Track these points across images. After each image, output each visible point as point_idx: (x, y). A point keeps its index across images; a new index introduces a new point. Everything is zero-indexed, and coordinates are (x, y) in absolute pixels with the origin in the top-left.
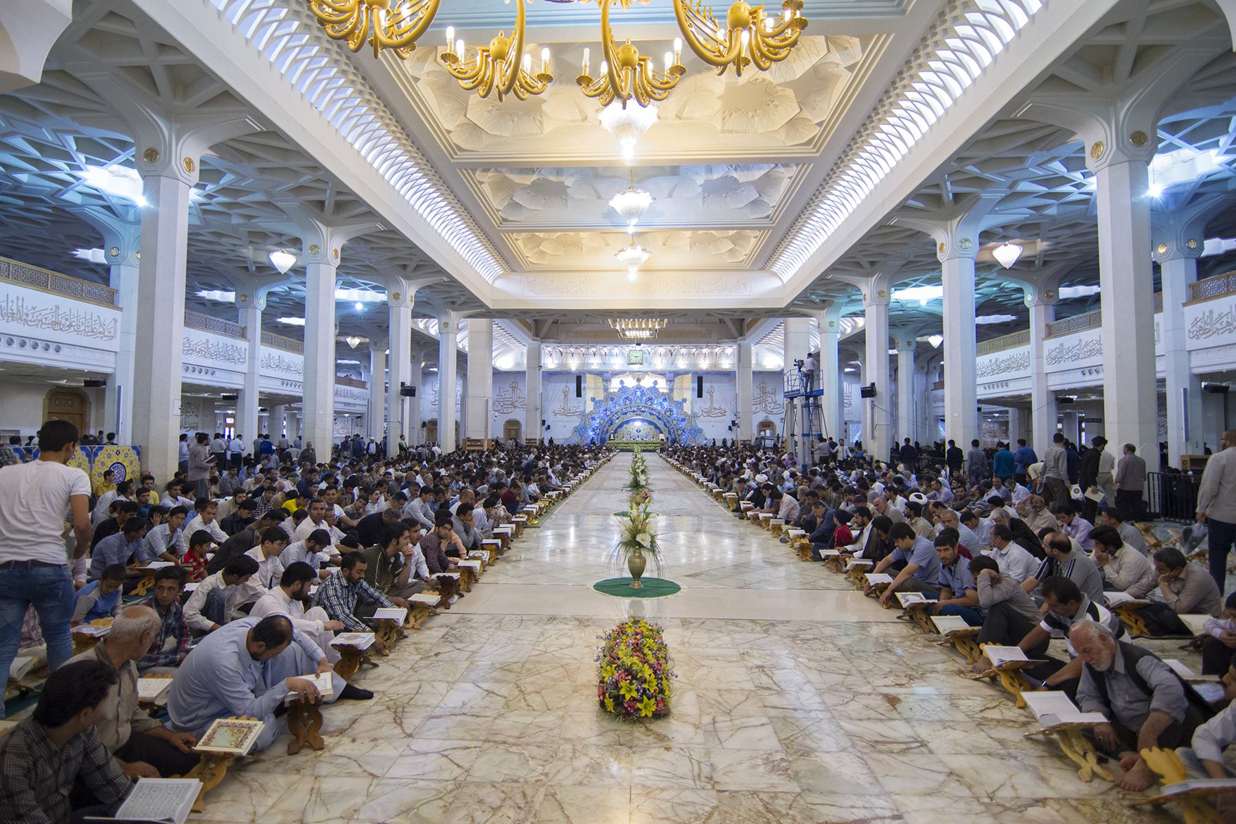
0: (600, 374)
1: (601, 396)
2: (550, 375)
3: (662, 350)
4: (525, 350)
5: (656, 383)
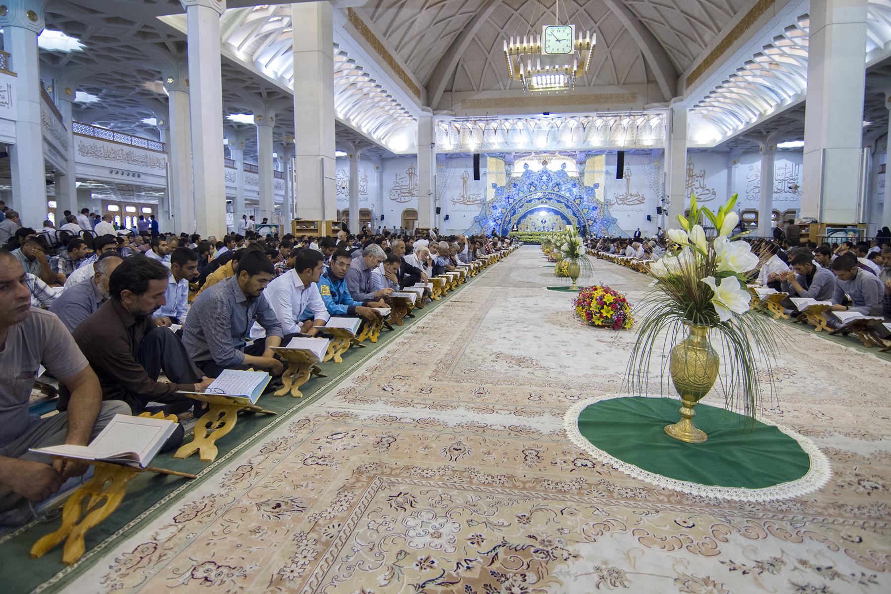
1: (503, 182)
2: (448, 159)
3: (573, 123)
4: (415, 126)
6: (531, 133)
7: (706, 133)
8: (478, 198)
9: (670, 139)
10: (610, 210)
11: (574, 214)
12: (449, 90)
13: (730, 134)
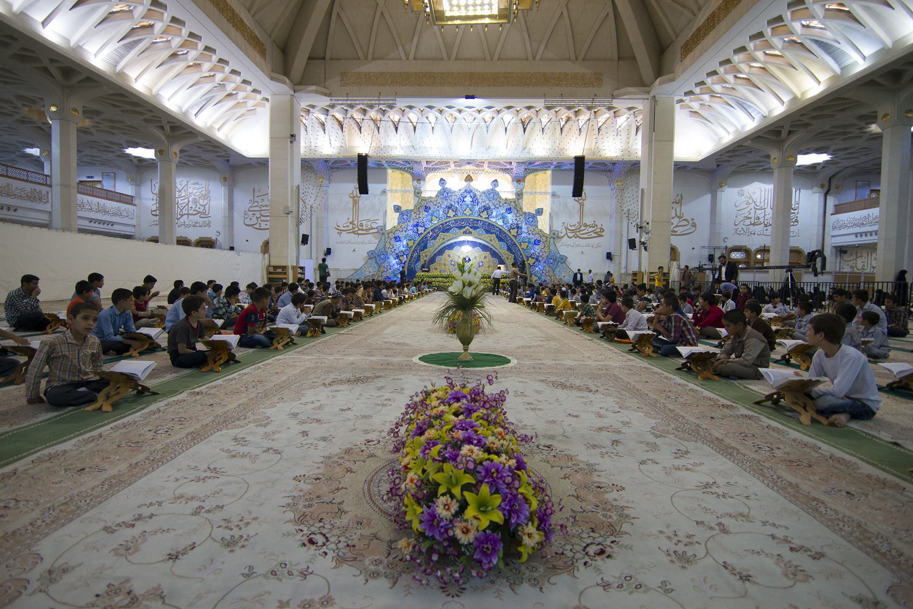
1: (409, 204)
8: (374, 226)
9: (650, 141)
10: (558, 245)
11: (509, 249)
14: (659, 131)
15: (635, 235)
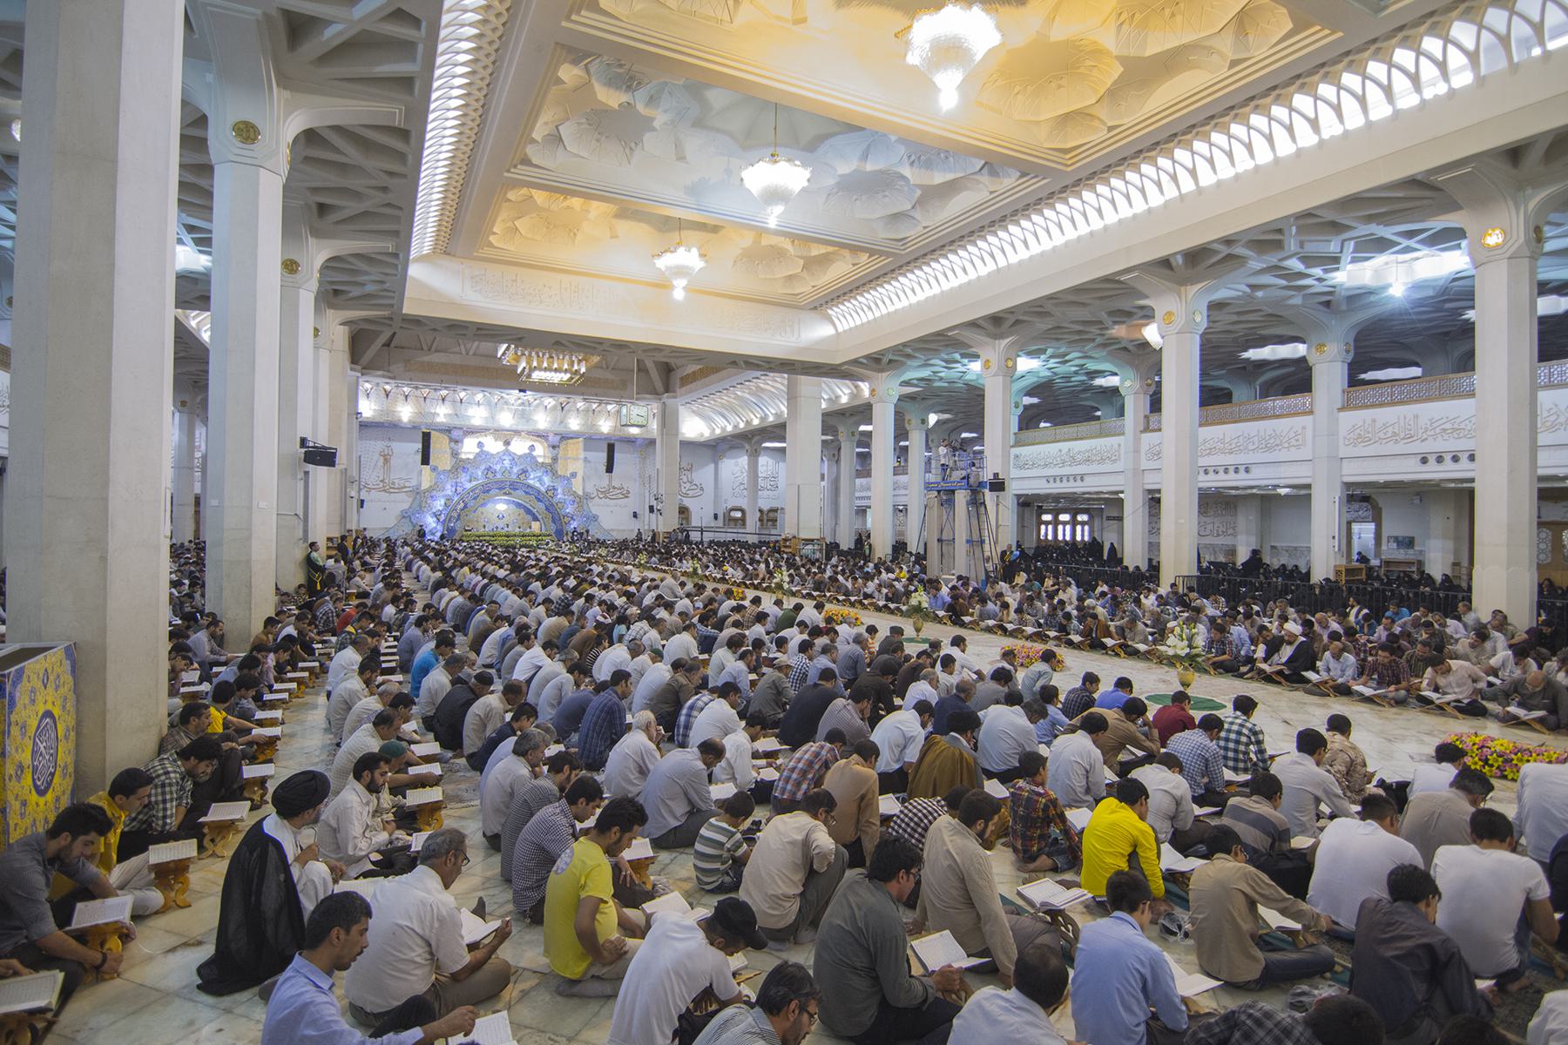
0: (448, 430)
5: (532, 448)
6: (493, 408)
7: (694, 427)
12: (387, 344)
13: (718, 431)
14: (669, 422)
15: (654, 503)
